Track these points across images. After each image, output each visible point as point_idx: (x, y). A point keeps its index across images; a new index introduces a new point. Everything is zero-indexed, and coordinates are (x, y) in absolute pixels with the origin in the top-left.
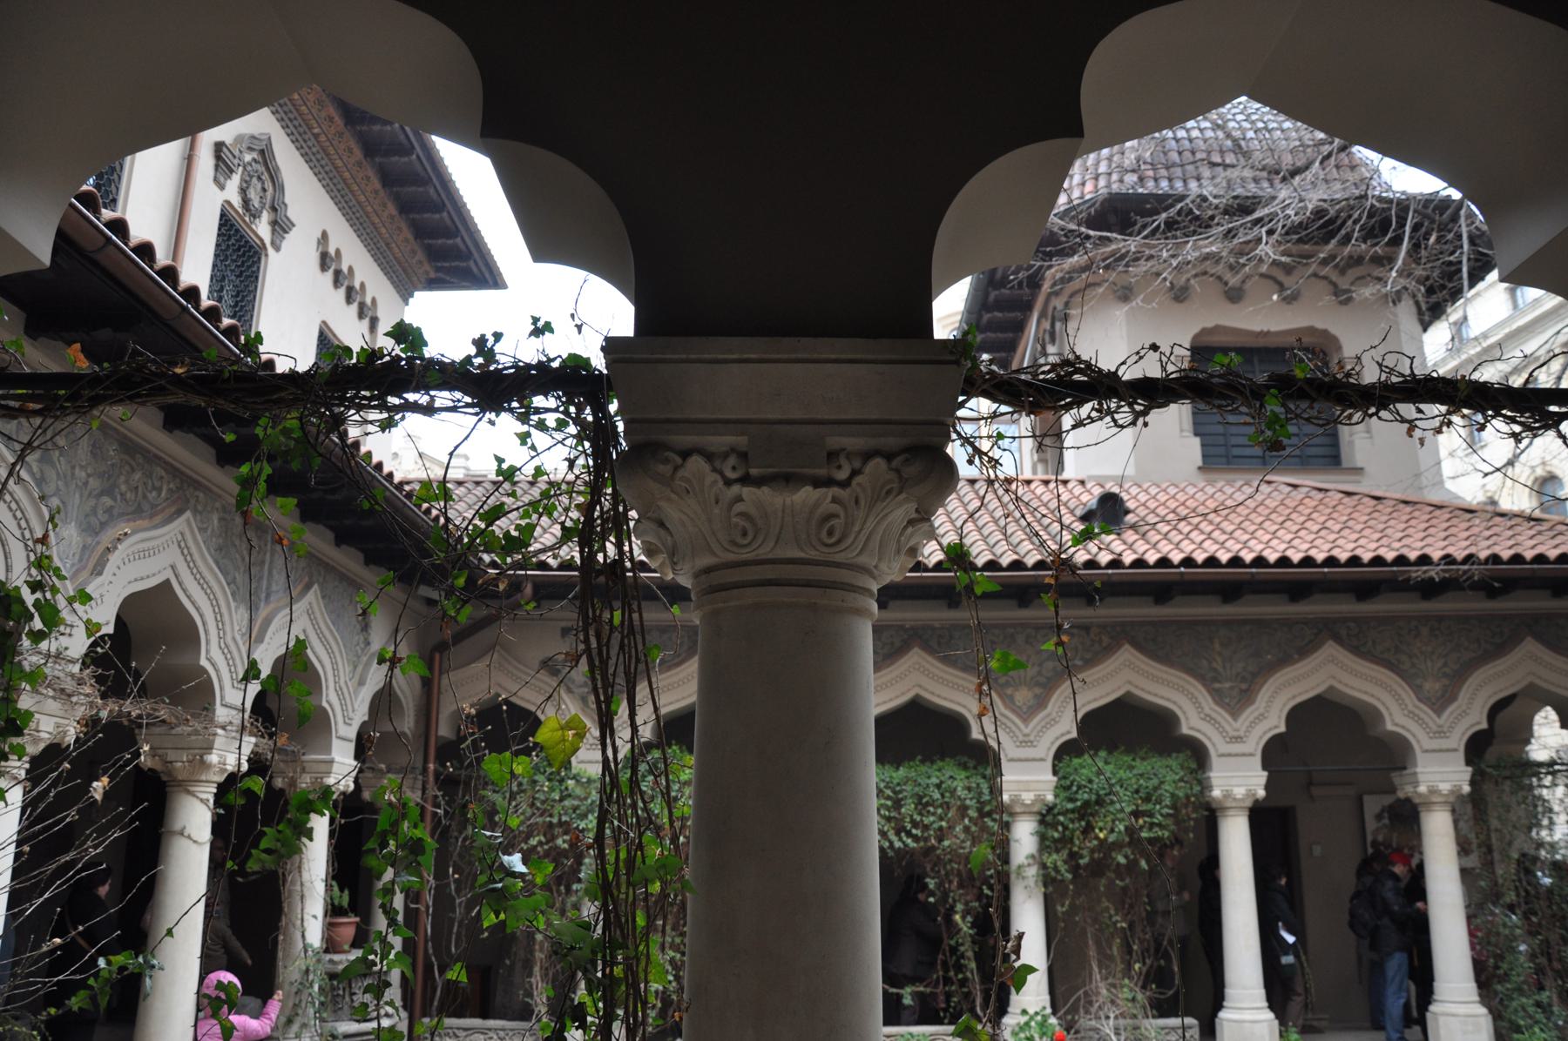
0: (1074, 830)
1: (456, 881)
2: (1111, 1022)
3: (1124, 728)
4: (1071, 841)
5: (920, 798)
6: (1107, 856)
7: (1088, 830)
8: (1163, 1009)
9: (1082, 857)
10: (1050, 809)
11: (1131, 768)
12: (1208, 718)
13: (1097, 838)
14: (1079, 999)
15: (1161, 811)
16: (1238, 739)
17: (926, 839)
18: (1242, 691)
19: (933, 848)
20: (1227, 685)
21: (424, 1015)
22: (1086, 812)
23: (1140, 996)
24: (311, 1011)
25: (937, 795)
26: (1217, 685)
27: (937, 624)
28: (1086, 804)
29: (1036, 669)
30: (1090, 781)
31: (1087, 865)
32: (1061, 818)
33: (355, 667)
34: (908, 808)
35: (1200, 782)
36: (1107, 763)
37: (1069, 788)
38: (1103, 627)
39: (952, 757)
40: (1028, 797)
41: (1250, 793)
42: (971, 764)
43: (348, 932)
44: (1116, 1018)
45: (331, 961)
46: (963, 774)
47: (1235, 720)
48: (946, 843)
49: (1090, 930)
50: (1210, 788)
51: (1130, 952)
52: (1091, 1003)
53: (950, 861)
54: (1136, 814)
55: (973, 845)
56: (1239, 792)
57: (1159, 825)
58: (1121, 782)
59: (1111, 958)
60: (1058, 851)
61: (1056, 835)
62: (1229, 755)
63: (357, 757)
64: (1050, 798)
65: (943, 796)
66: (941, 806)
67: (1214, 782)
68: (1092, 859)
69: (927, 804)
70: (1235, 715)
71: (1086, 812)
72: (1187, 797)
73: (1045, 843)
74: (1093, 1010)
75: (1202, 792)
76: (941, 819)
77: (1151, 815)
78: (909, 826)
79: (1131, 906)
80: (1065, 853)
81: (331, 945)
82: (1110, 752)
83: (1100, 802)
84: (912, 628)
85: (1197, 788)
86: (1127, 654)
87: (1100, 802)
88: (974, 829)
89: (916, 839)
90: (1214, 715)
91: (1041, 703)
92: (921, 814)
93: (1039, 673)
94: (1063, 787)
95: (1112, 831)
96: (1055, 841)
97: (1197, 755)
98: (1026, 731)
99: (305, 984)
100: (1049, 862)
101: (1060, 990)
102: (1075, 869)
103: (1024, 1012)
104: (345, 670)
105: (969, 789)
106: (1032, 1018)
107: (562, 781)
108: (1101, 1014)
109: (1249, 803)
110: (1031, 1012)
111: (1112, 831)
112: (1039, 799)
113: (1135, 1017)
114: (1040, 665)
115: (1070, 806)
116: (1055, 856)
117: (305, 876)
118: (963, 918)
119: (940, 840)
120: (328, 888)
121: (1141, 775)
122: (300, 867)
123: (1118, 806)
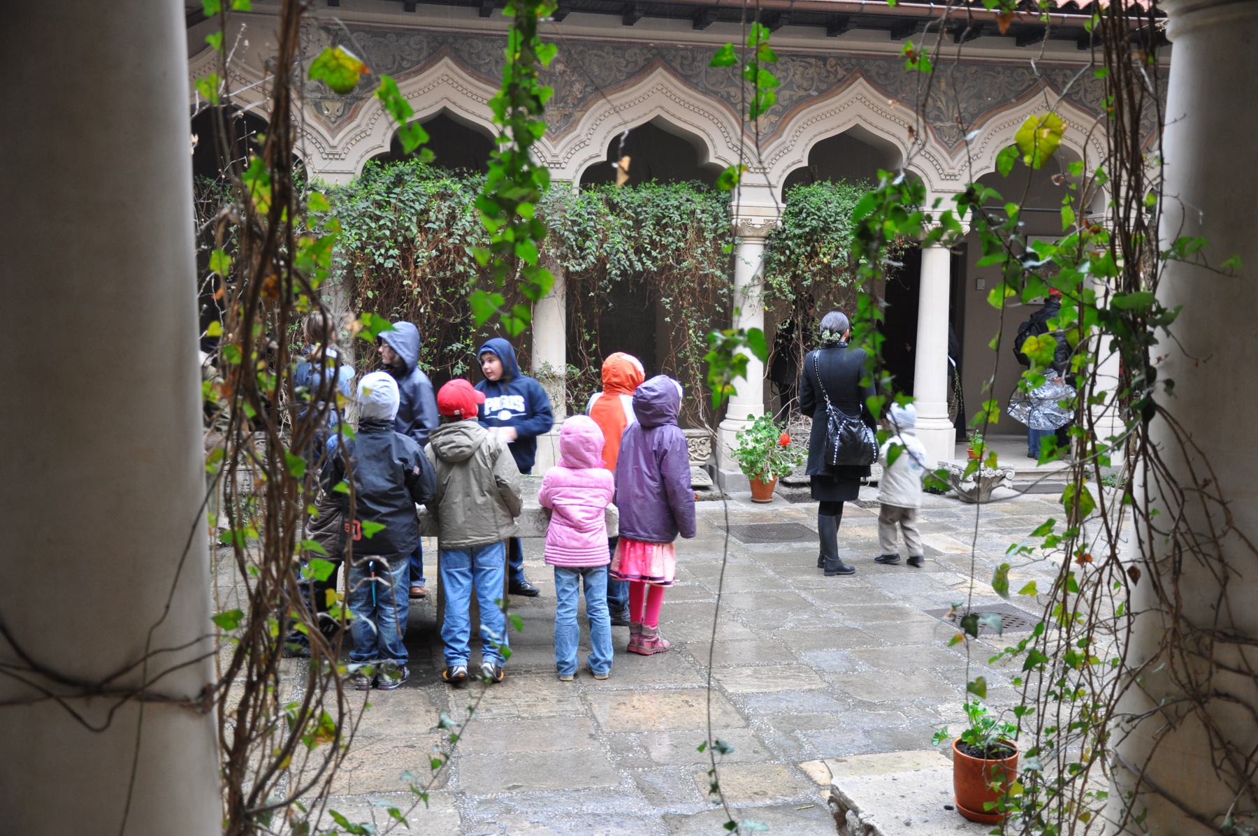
4: (796, 265)
7: (813, 255)
13: (820, 262)
20: (949, 124)
22: (811, 238)
26: (939, 124)
28: (814, 230)
32: (790, 243)
38: (840, 58)
60: (782, 273)
69: (666, 225)
71: (811, 238)
76: (679, 240)
80: (788, 276)
84: (656, 47)
86: (860, 87)
111: (836, 257)
115: (798, 231)
116: (780, 278)
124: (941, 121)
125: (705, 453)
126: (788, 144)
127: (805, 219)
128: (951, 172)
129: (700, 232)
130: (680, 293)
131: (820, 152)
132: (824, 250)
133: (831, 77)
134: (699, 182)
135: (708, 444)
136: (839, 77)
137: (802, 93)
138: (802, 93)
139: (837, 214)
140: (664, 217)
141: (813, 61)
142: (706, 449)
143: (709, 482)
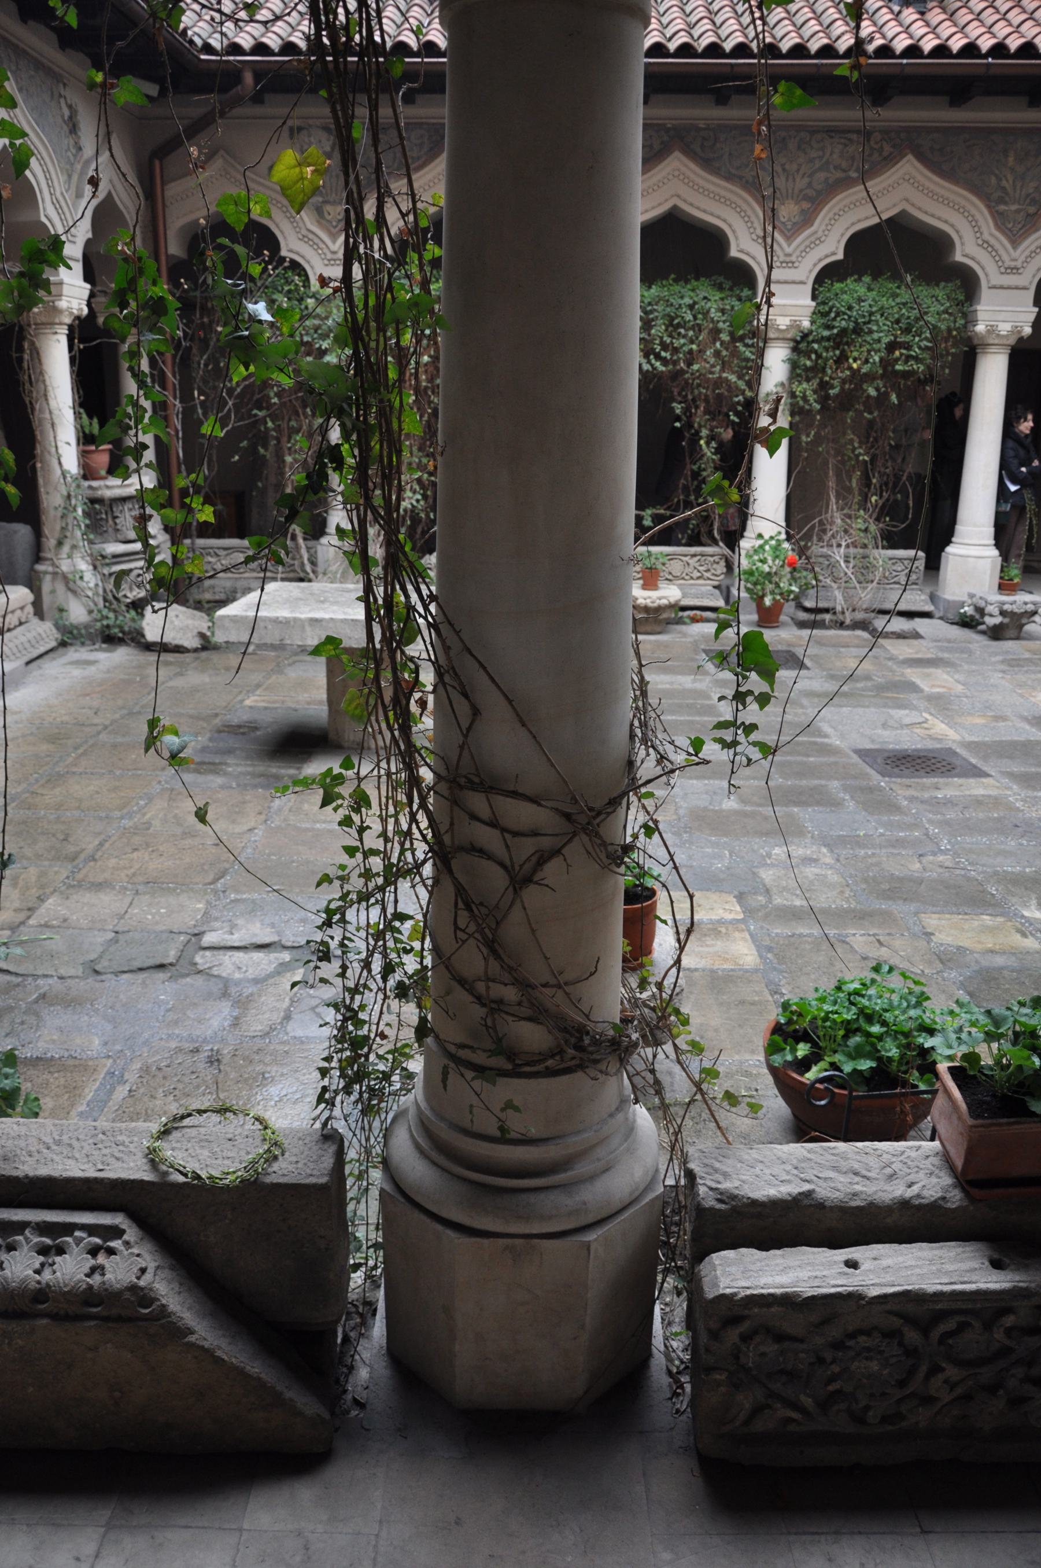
0: (827, 359)
1: (202, 403)
2: (842, 550)
3: (896, 251)
5: (672, 319)
6: (859, 387)
8: (892, 541)
9: (833, 387)
10: (805, 336)
11: (895, 296)
12: (986, 245)
13: (850, 368)
14: (813, 527)
15: (920, 343)
16: (1014, 270)
17: (675, 363)
18: (1028, 215)
19: (682, 372)
21: (186, 537)
22: (841, 341)
23: (873, 528)
24: (78, 534)
25: (689, 317)
27: (702, 124)
28: (844, 331)
29: (806, 180)
30: (850, 308)
31: (837, 396)
32: (816, 346)
33: (70, 176)
34: (659, 329)
35: (965, 315)
36: (870, 289)
37: (828, 313)
39: (708, 276)
40: (783, 322)
41: (1016, 330)
42: (727, 285)
43: (102, 459)
44: (847, 546)
45: (90, 487)
46: (718, 295)
47: (1015, 248)
48: (696, 367)
49: (832, 462)
50: (975, 322)
51: (868, 484)
52: (824, 531)
53: (699, 385)
54: (891, 347)
55: (723, 370)
56: (1005, 328)
57: (916, 359)
58: (882, 311)
59: (849, 490)
60: (808, 380)
61: (808, 363)
62: (1002, 287)
63: (86, 279)
64: (806, 324)
65: (695, 318)
66: (693, 328)
67: (980, 316)
68: (842, 389)
69: (679, 326)
70: (1015, 243)
71: (841, 341)
72: (949, 330)
73: (796, 371)
74: (826, 538)
75: (965, 326)
76: (692, 342)
77: (908, 347)
78: (658, 348)
79: (876, 440)
80: (815, 382)
81: (88, 473)
82: (875, 278)
83: (857, 331)
85: (961, 322)
86: (909, 166)
87: (857, 331)
88: (724, 353)
89: (665, 362)
90: (993, 241)
91: (807, 219)
92: (670, 336)
93: (809, 185)
94: (821, 313)
95: (867, 361)
96: (807, 369)
97: (967, 284)
98: (788, 250)
99: (68, 508)
100: (798, 389)
101: (797, 517)
102: (824, 400)
103: (760, 536)
104: (59, 181)
105: (723, 311)
106: (766, 542)
107: (301, 300)
108: (834, 542)
109: (1012, 341)
110: (767, 537)
111: (867, 361)
112: (795, 325)
113: (865, 546)
114: (811, 175)
115: (826, 333)
116: (805, 385)
117: (53, 403)
118: (708, 444)
119: (689, 364)
120: (77, 416)
121: (904, 304)
122: (46, 395)
123: (876, 336)
124: (1006, 203)
125: (719, 572)
126: (820, 233)
127: (834, 319)
128: (1013, 264)
129: (715, 332)
130: (694, 400)
131: (857, 243)
132: (856, 354)
133: (873, 154)
134: (721, 279)
135: (723, 563)
136: (885, 154)
137: (839, 174)
138: (839, 174)
139: (871, 314)
140: (677, 316)
141: (854, 137)
142: (721, 568)
143: (721, 603)
